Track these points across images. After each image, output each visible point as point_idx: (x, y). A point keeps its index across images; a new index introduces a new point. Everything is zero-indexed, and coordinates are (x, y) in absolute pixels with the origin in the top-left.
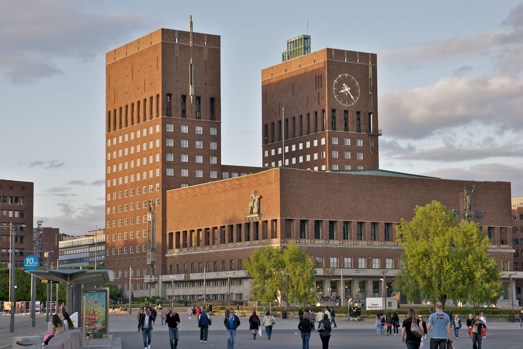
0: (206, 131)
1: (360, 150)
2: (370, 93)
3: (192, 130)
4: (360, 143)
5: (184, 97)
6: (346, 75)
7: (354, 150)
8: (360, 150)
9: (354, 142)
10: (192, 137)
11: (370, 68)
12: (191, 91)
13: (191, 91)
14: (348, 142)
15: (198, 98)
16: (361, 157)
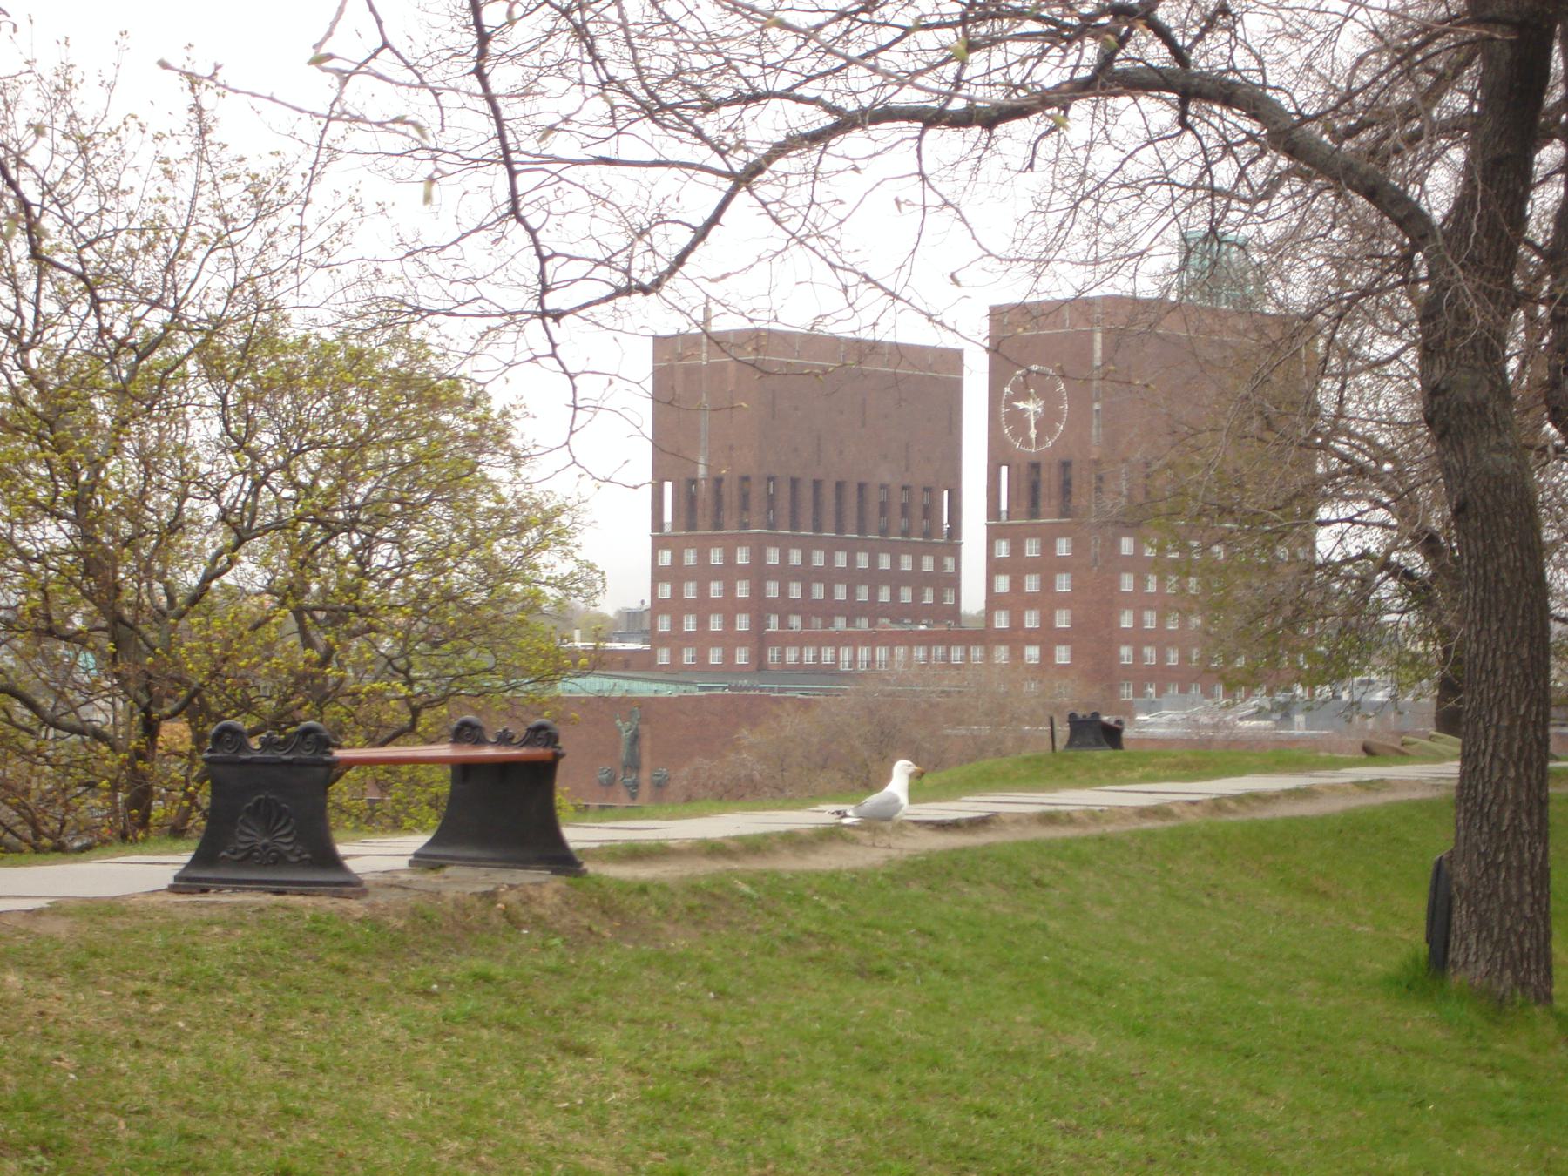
0: (729, 558)
1: (1063, 565)
2: (1097, 406)
3: (703, 556)
4: (1063, 547)
5: (694, 481)
6: (1035, 368)
7: (1048, 566)
8: (1063, 565)
9: (1048, 547)
10: (704, 574)
11: (1098, 337)
12: (702, 471)
13: (702, 471)
14: (1032, 549)
15: (719, 481)
16: (1063, 584)
